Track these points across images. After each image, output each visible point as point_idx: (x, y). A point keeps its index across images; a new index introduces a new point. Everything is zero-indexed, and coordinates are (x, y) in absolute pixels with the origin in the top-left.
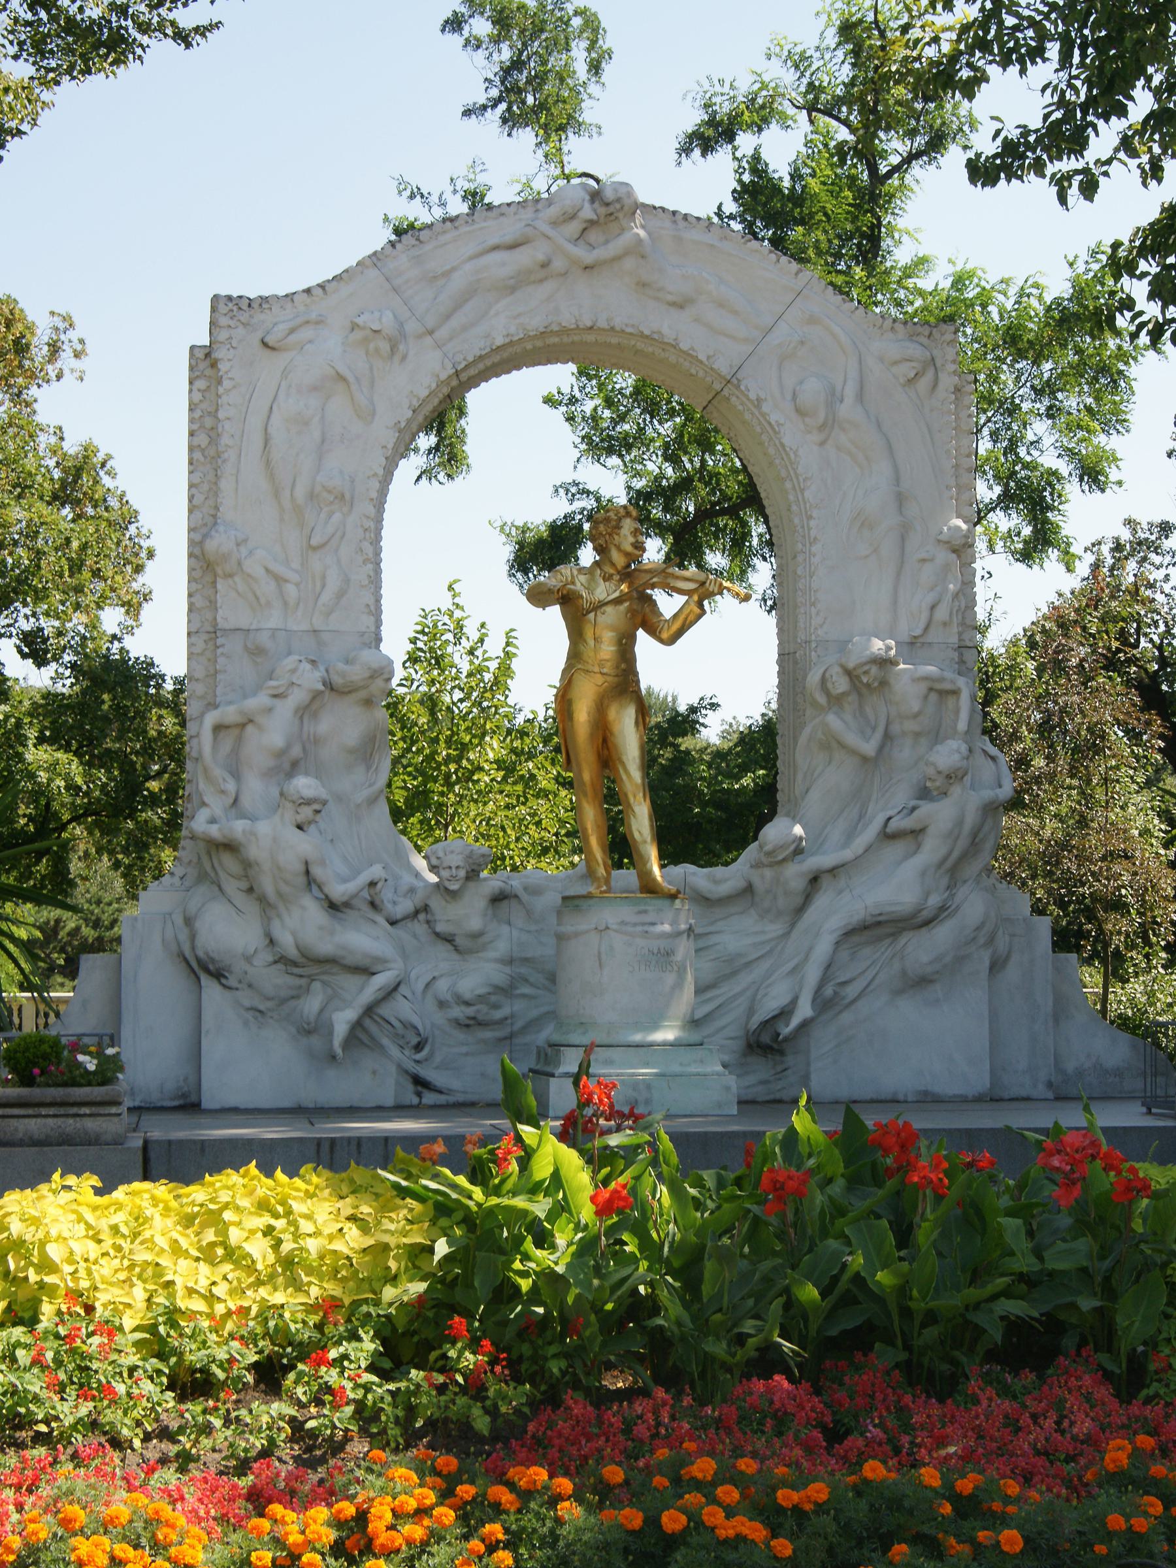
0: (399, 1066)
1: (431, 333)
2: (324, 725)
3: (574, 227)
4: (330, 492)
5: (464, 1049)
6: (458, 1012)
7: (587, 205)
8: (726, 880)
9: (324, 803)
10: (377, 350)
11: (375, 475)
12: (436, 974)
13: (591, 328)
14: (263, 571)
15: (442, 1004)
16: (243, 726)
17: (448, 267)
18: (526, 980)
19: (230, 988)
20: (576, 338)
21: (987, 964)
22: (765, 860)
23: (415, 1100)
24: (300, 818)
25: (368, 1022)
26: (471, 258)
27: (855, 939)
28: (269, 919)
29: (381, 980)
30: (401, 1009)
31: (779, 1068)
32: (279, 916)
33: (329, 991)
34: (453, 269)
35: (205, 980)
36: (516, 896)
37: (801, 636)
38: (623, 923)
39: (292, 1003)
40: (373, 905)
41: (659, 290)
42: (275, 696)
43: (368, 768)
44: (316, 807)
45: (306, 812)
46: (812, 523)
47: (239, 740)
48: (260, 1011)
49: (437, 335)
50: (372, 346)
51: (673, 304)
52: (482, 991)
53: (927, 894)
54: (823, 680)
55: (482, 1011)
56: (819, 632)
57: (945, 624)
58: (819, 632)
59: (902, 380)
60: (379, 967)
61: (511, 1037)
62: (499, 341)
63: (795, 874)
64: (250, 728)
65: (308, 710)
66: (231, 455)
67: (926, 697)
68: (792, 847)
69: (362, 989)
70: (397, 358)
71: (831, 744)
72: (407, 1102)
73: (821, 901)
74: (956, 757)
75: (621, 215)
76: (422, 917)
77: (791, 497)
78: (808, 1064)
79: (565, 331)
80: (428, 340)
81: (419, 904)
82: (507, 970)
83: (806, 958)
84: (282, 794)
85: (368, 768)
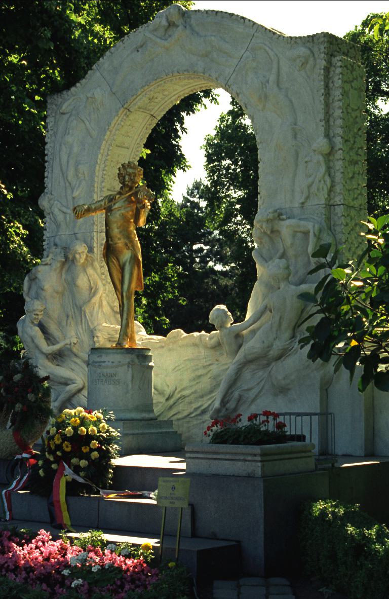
3: (161, 32)
27: (253, 366)
29: (72, 388)
67: (294, 236)
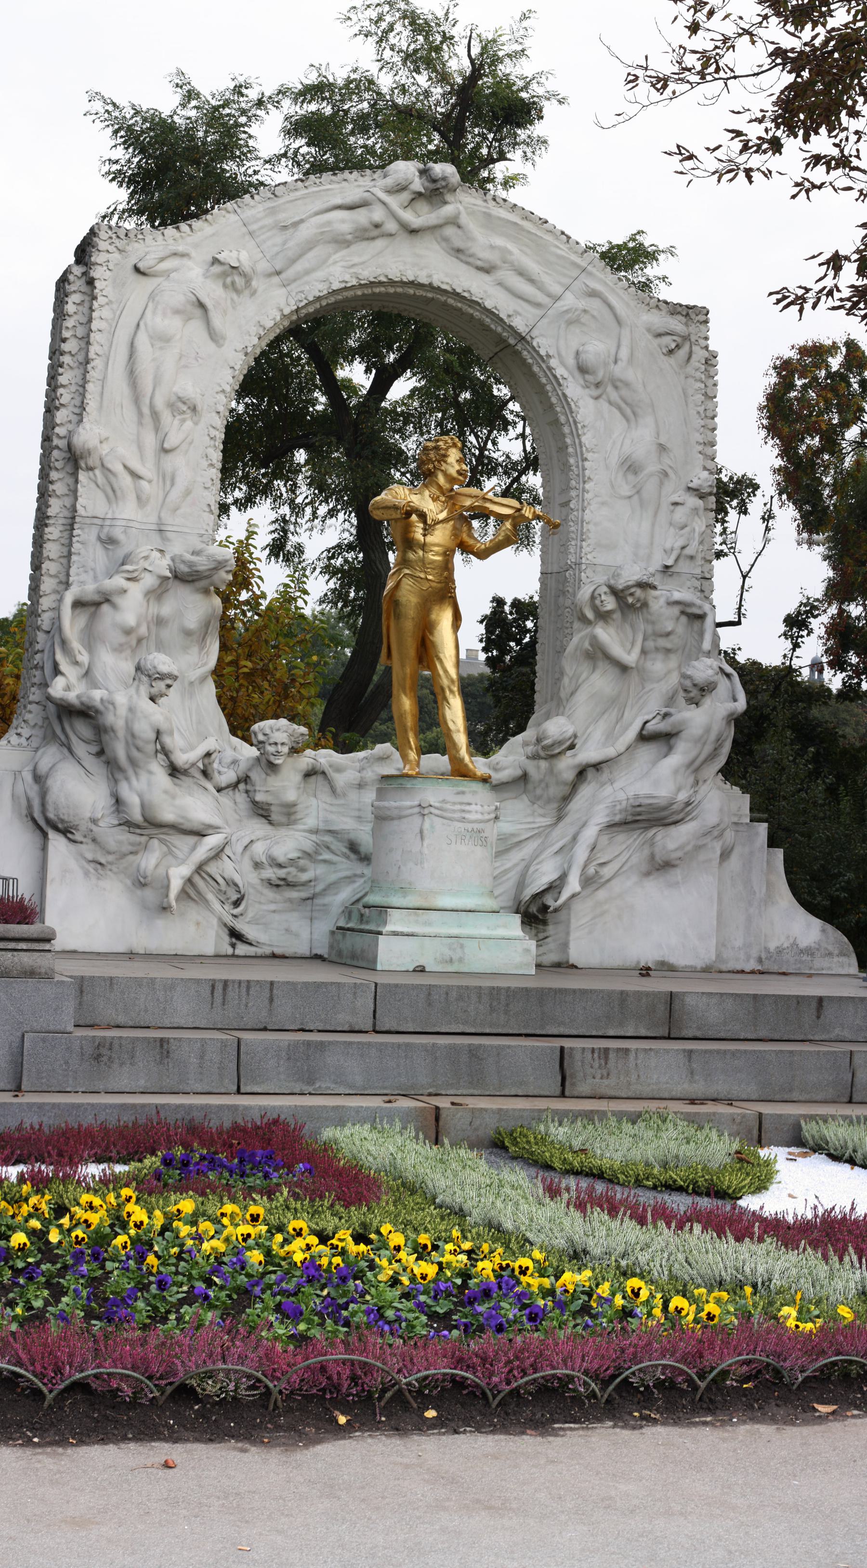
0: (220, 919)
1: (278, 273)
2: (167, 609)
3: (406, 196)
4: (184, 403)
5: (273, 907)
6: (270, 873)
7: (417, 180)
8: (505, 769)
9: (175, 678)
10: (233, 283)
11: (223, 391)
12: (253, 838)
13: (412, 283)
14: (121, 468)
15: (257, 865)
16: (98, 604)
17: (297, 219)
18: (328, 848)
19: (75, 842)
20: (399, 290)
21: (719, 853)
22: (542, 754)
23: (230, 951)
24: (154, 691)
25: (197, 879)
26: (317, 214)
28: (116, 781)
30: (227, 868)
31: (541, 936)
32: (127, 779)
33: (165, 849)
34: (302, 221)
35: (52, 834)
36: (323, 773)
37: (572, 559)
38: (444, 801)
39: (131, 858)
40: (205, 773)
41: (471, 256)
42: (129, 579)
43: (201, 649)
44: (169, 682)
45: (160, 686)
46: (587, 464)
47: (93, 617)
48: (100, 864)
49: (283, 276)
50: (229, 280)
51: (479, 269)
52: (294, 855)
53: (679, 790)
54: (593, 597)
55: (291, 873)
56: (589, 556)
57: (692, 558)
58: (589, 556)
59: (664, 351)
60: (210, 832)
61: (311, 898)
62: (336, 286)
63: (567, 765)
64: (105, 608)
65: (157, 593)
66: (97, 363)
67: (678, 619)
68: (568, 743)
69: (194, 848)
70: (247, 292)
71: (598, 654)
72: (224, 953)
73: (586, 791)
74: (710, 672)
75: (445, 191)
76: (242, 786)
77: (568, 441)
78: (568, 934)
79: (392, 283)
80: (276, 280)
81: (241, 774)
82: (314, 837)
83: (574, 839)
84: (138, 668)
85: (201, 649)
